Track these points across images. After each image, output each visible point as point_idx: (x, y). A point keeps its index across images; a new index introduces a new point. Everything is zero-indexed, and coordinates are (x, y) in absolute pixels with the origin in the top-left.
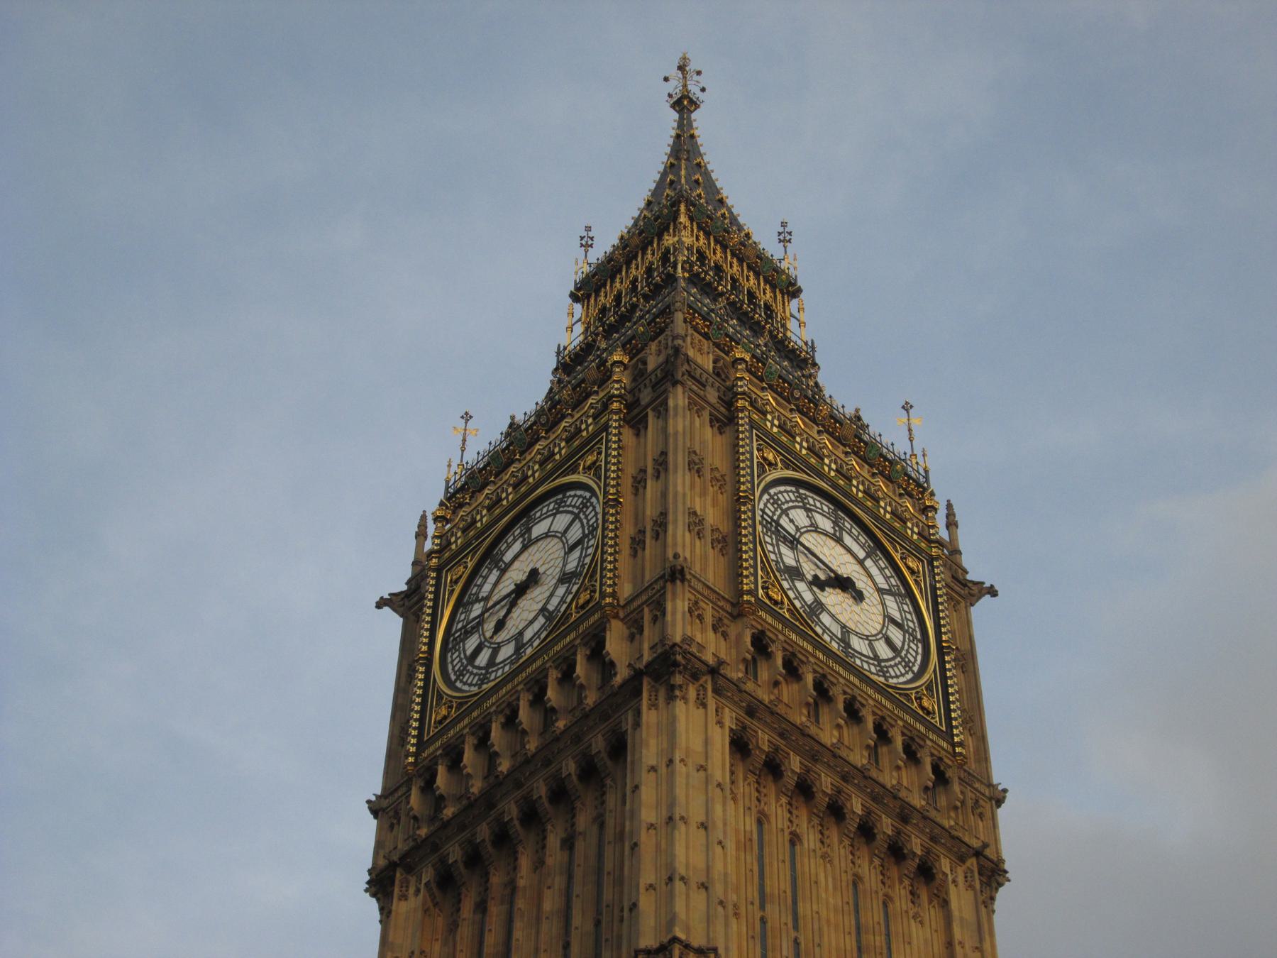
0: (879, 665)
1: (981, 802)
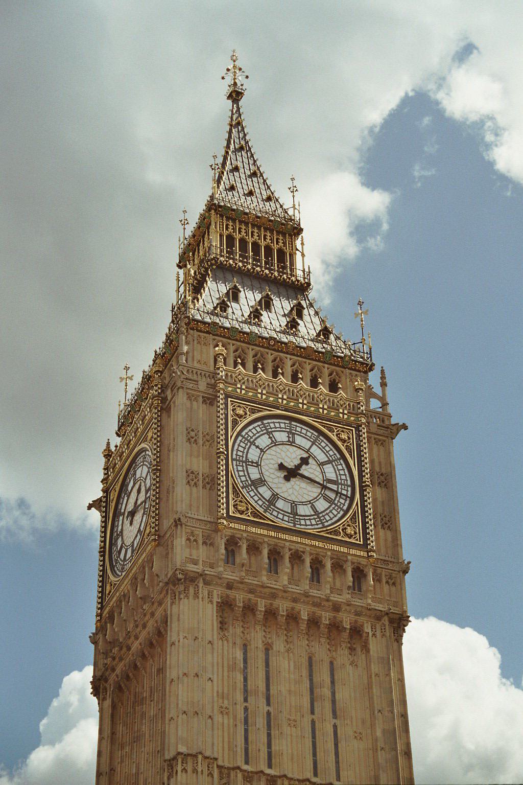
0: (319, 517)
1: (394, 575)
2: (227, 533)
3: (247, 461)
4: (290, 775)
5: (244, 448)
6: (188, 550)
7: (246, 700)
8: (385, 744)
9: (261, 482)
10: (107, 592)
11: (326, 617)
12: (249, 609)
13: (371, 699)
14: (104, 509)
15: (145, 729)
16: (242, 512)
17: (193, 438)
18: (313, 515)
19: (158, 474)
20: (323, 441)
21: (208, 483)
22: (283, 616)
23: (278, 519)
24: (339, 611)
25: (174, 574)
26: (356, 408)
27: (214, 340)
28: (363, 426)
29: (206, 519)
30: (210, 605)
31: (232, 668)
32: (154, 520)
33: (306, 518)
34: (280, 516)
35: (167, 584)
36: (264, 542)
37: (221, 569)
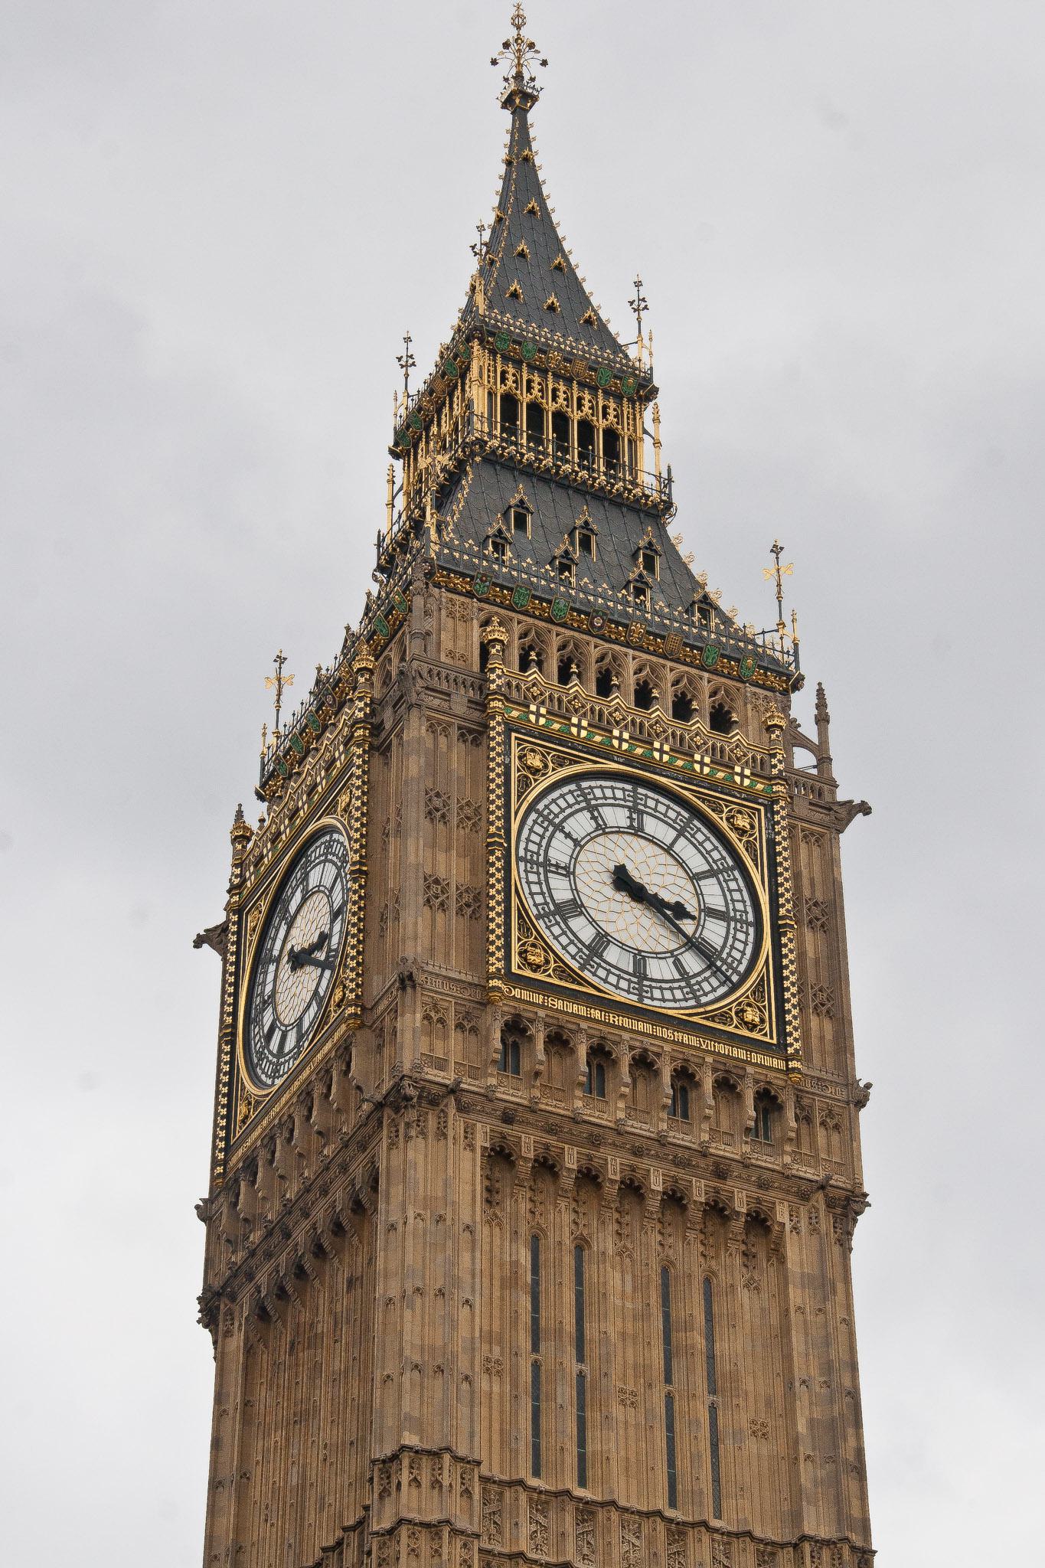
0: (689, 985)
2: (505, 1009)
3: (547, 864)
4: (622, 1503)
5: (542, 837)
6: (425, 1039)
7: (535, 1348)
8: (814, 1449)
9: (575, 907)
10: (239, 1118)
11: (699, 1191)
12: (546, 1166)
13: (788, 1358)
14: (233, 948)
15: (322, 1396)
16: (536, 968)
17: (438, 810)
18: (678, 981)
19: (363, 882)
20: (699, 830)
21: (468, 905)
22: (612, 1181)
23: (607, 986)
24: (725, 1179)
25: (397, 1087)
26: (767, 766)
27: (481, 610)
28: (782, 803)
29: (463, 977)
30: (468, 1154)
31: (511, 1281)
32: (353, 975)
33: (664, 985)
34: (613, 979)
35: (379, 1106)
36: (580, 1030)
37: (493, 1081)
